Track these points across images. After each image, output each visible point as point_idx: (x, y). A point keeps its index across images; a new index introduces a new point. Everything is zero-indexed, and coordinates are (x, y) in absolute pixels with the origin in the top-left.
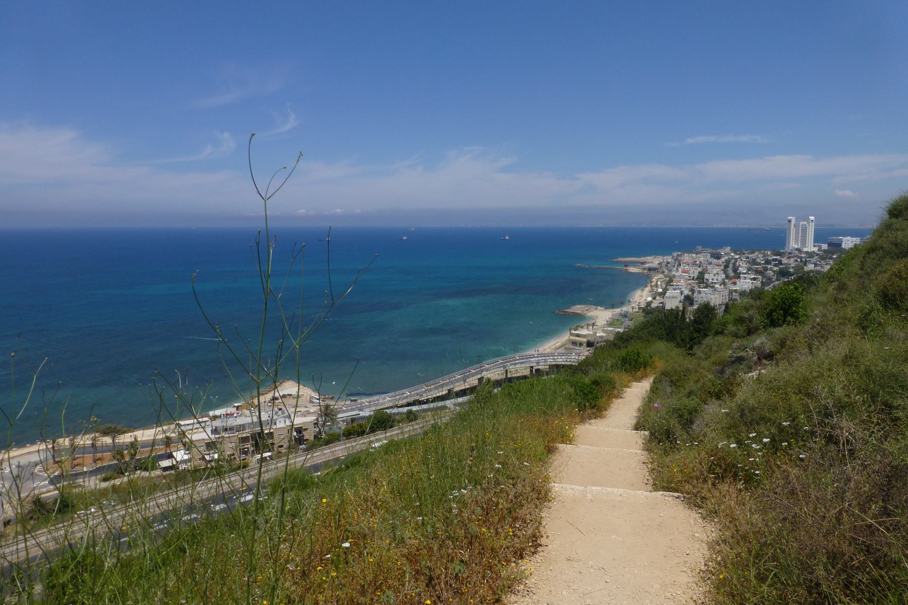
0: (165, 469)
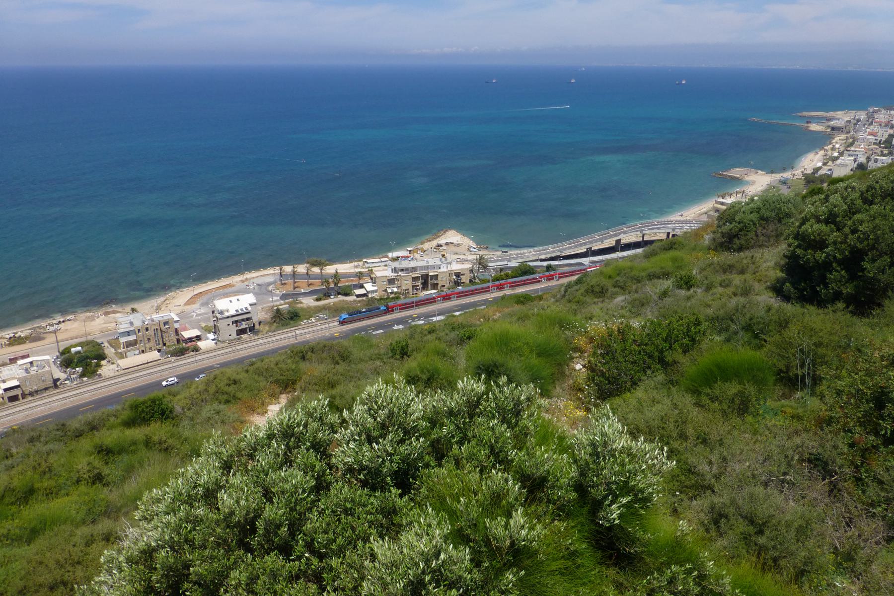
0: (358, 296)
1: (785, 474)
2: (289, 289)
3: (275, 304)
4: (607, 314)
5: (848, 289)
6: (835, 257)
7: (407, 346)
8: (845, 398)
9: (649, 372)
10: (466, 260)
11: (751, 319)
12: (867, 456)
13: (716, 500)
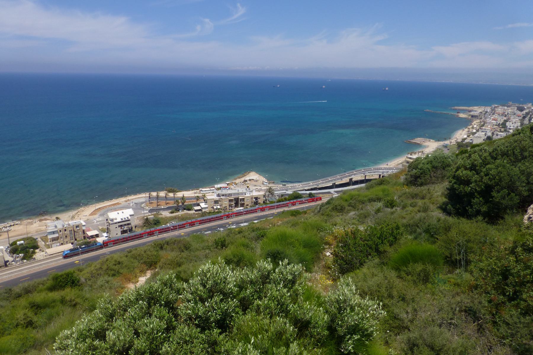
0: (196, 211)
1: (451, 319)
2: (154, 206)
3: (145, 215)
4: (345, 222)
5: (484, 209)
6: (476, 190)
7: (225, 240)
8: (485, 273)
9: (370, 257)
10: (261, 190)
11: (429, 226)
12: (499, 308)
13: (411, 335)
